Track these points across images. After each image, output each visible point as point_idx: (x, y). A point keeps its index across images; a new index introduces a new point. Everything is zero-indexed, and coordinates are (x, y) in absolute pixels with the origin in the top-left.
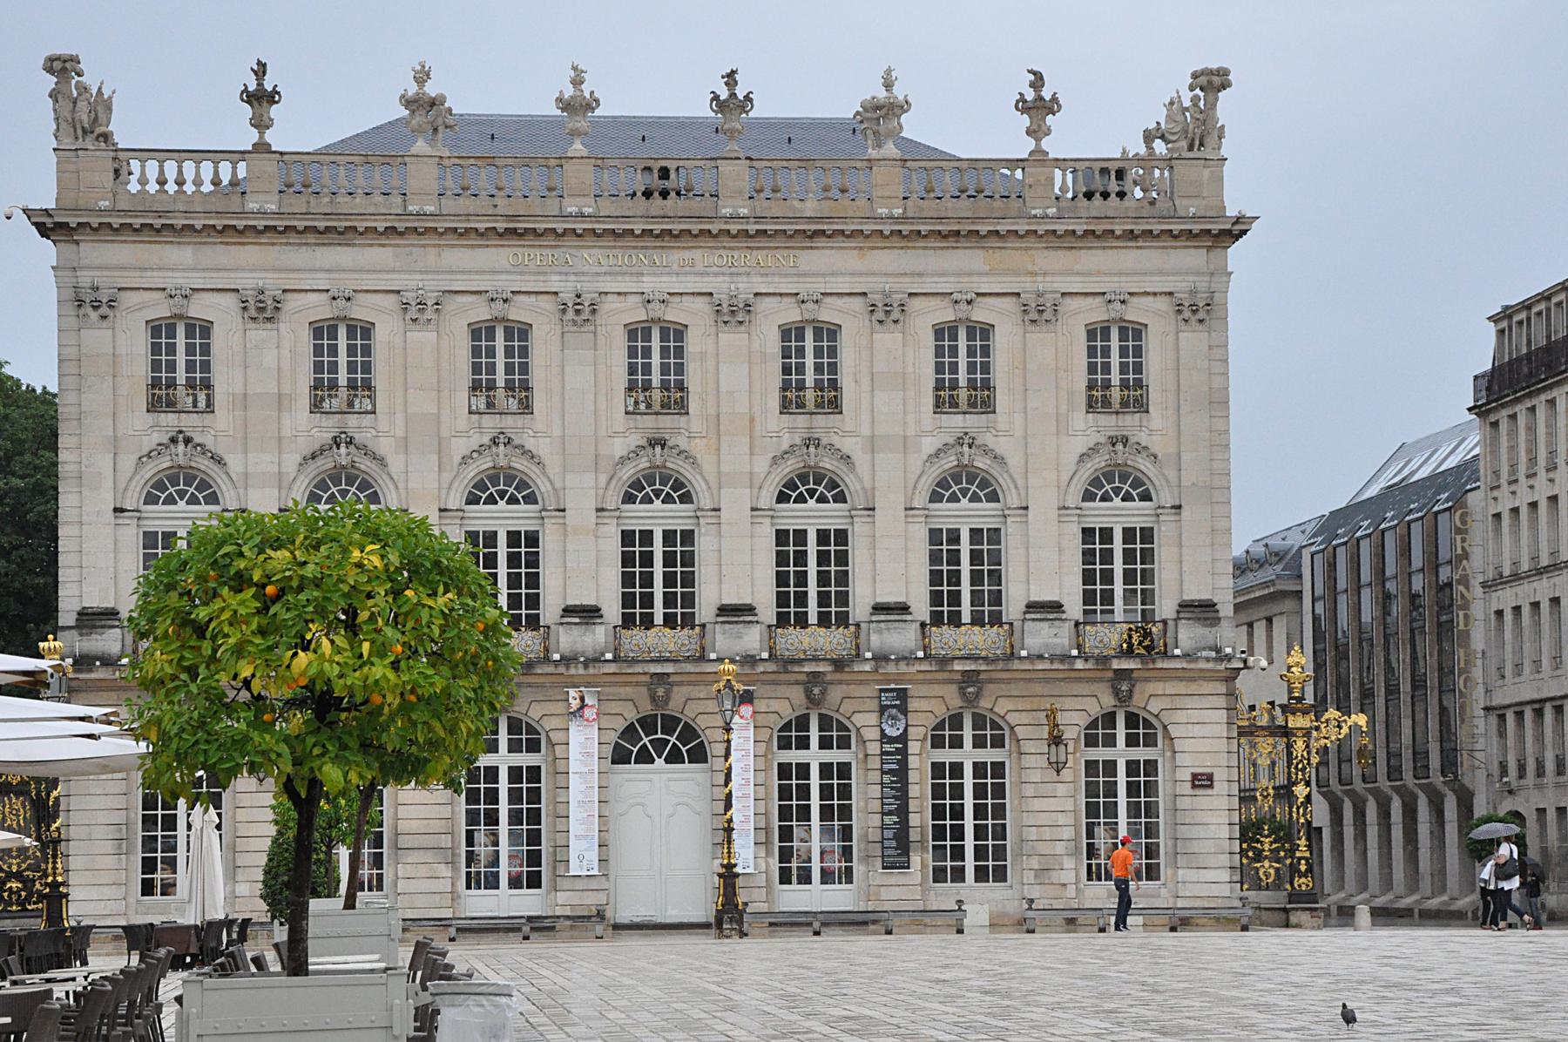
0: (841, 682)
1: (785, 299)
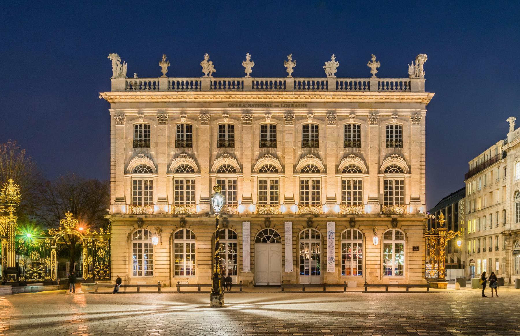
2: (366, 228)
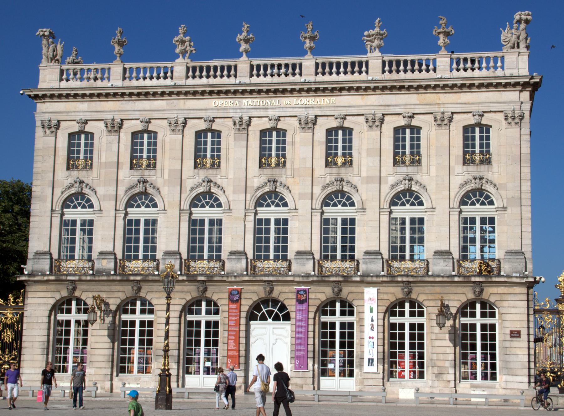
1: (330, 118)
2: (430, 297)
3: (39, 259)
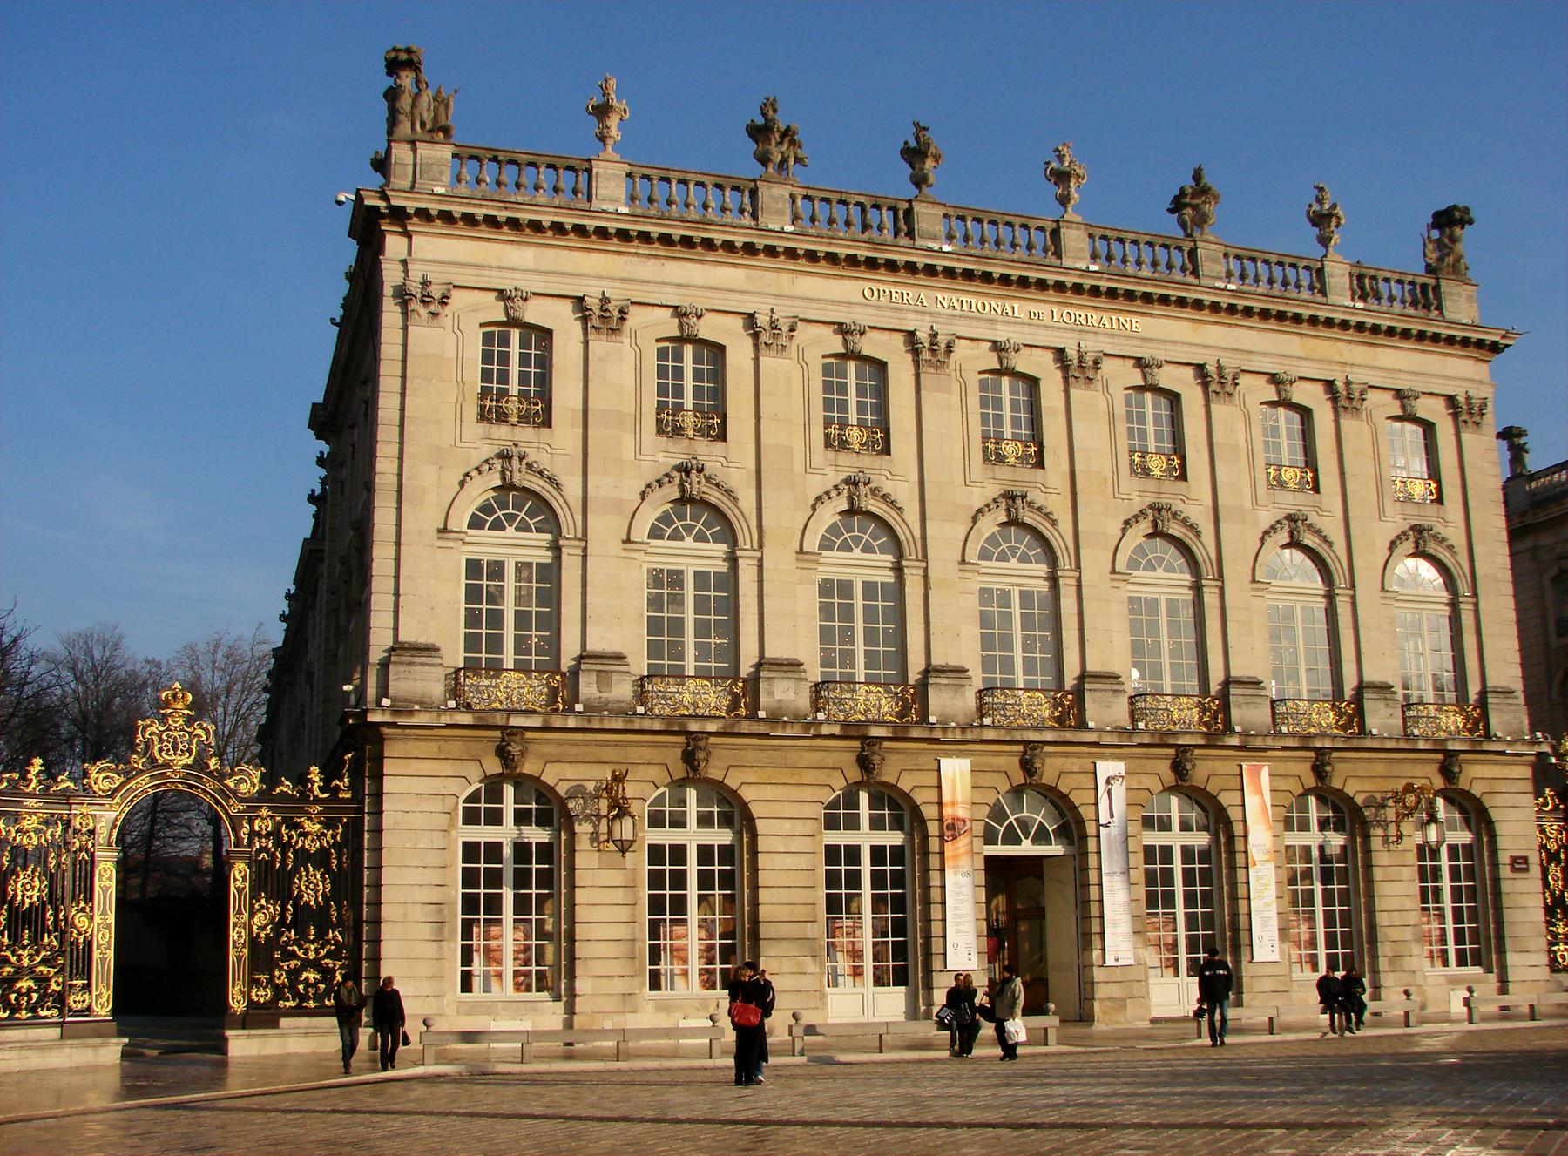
0: (1207, 757)
3: (410, 664)
